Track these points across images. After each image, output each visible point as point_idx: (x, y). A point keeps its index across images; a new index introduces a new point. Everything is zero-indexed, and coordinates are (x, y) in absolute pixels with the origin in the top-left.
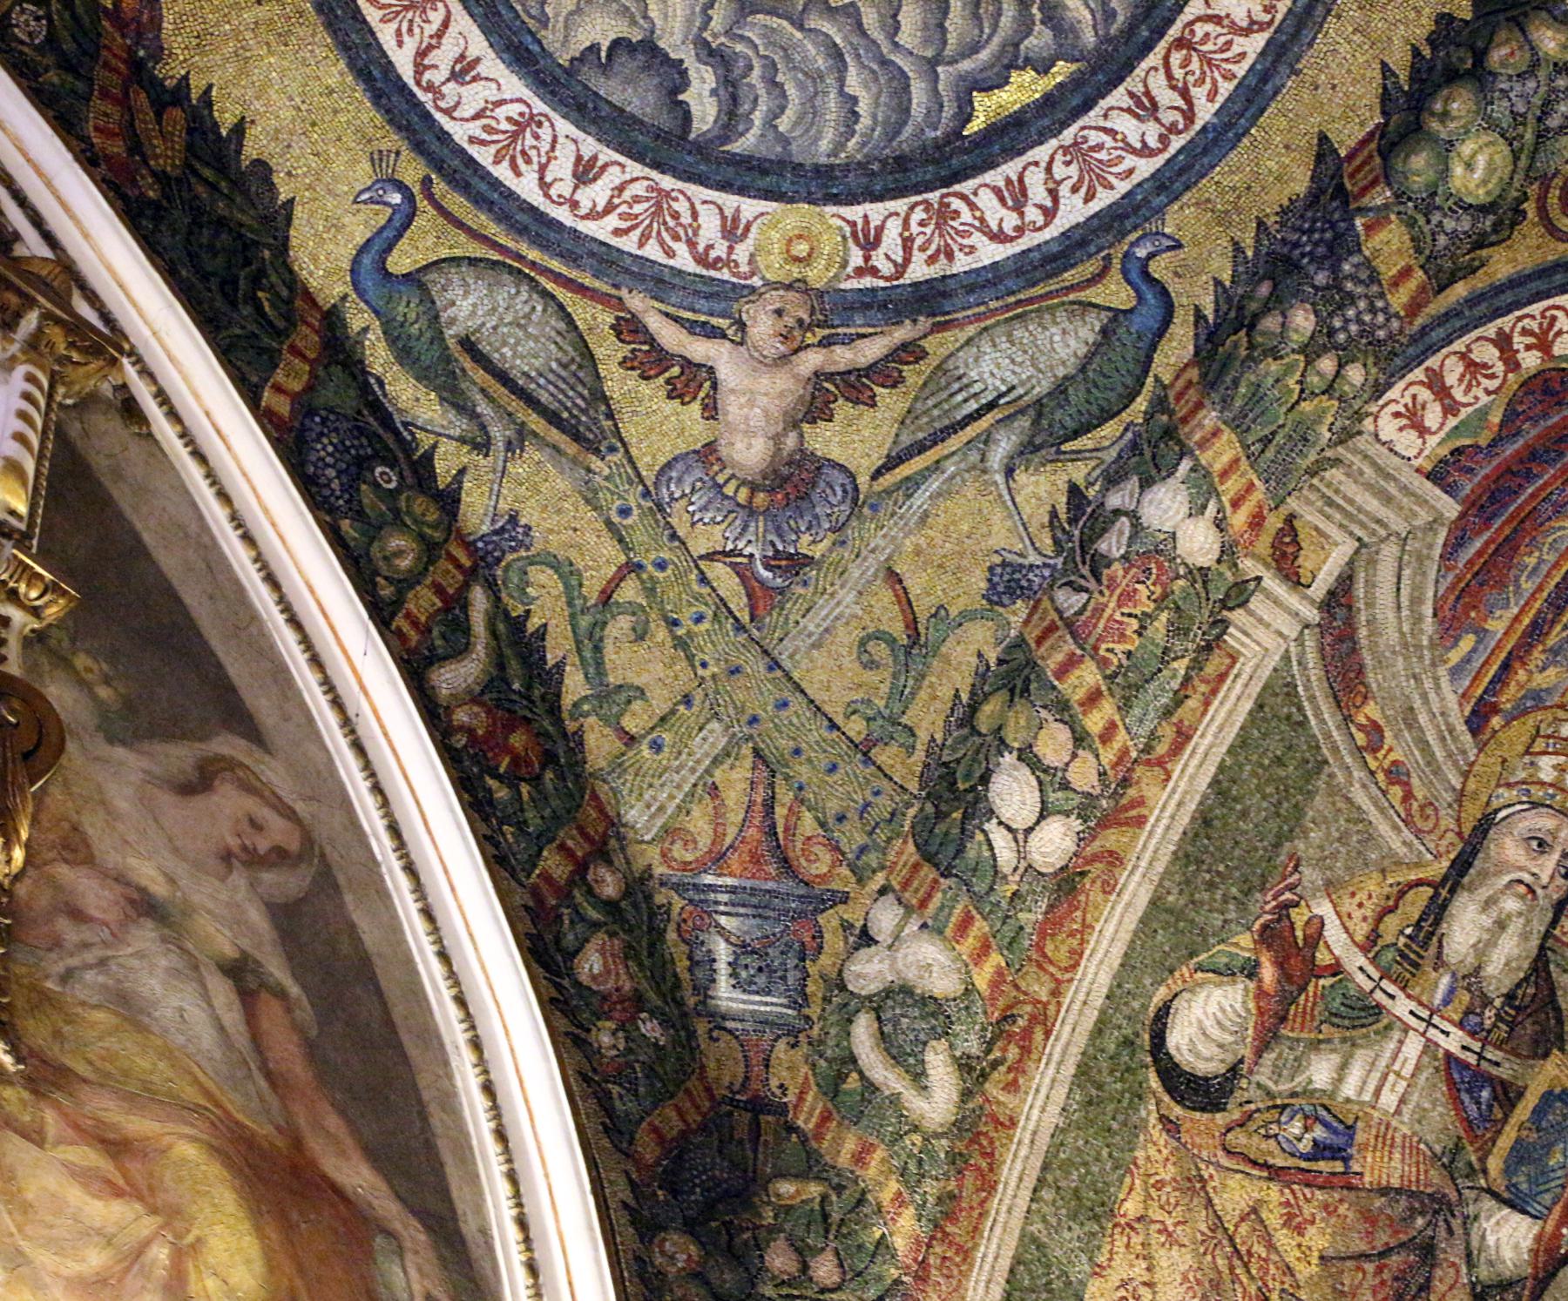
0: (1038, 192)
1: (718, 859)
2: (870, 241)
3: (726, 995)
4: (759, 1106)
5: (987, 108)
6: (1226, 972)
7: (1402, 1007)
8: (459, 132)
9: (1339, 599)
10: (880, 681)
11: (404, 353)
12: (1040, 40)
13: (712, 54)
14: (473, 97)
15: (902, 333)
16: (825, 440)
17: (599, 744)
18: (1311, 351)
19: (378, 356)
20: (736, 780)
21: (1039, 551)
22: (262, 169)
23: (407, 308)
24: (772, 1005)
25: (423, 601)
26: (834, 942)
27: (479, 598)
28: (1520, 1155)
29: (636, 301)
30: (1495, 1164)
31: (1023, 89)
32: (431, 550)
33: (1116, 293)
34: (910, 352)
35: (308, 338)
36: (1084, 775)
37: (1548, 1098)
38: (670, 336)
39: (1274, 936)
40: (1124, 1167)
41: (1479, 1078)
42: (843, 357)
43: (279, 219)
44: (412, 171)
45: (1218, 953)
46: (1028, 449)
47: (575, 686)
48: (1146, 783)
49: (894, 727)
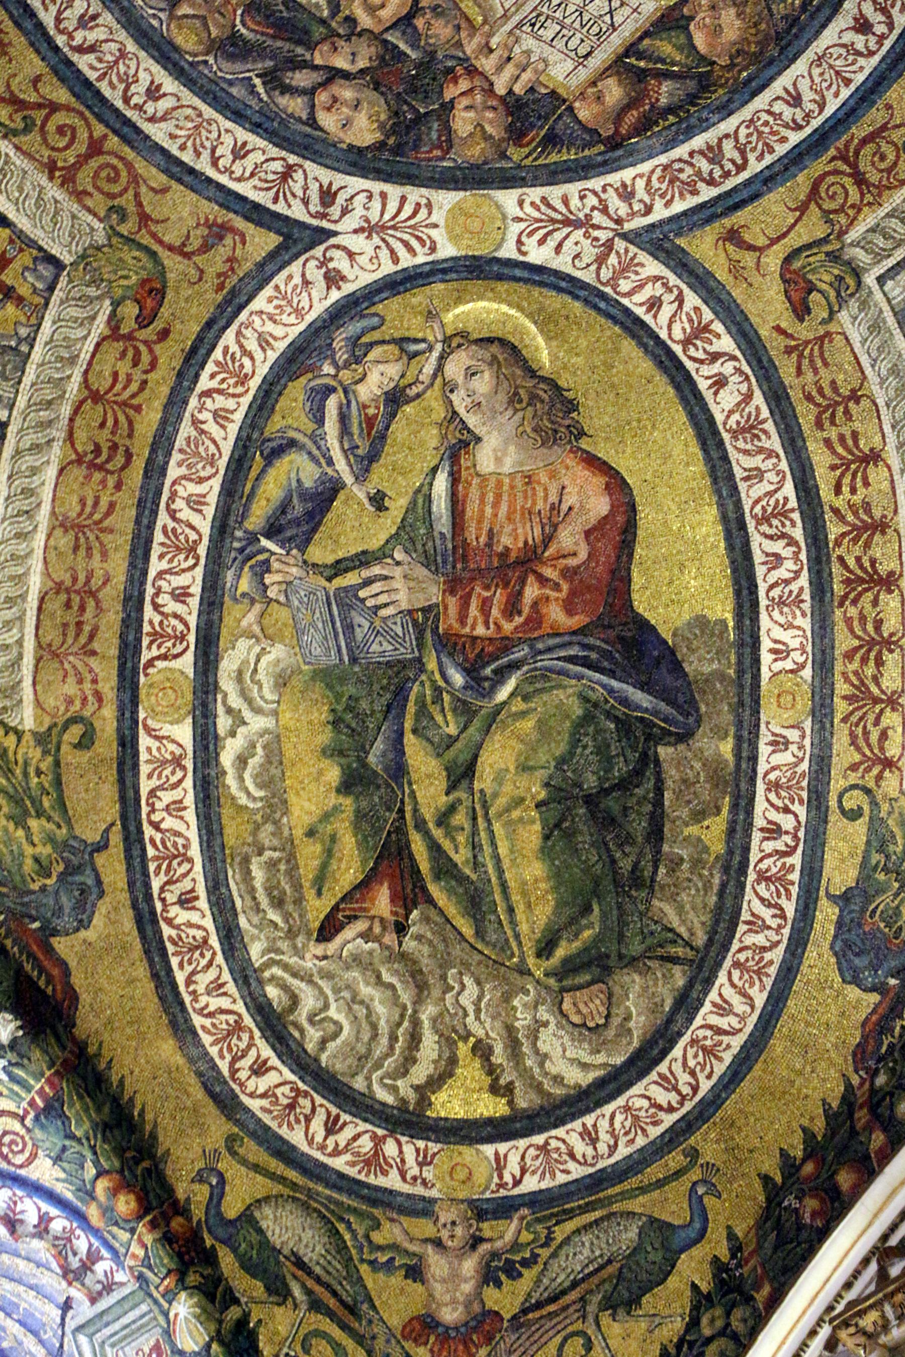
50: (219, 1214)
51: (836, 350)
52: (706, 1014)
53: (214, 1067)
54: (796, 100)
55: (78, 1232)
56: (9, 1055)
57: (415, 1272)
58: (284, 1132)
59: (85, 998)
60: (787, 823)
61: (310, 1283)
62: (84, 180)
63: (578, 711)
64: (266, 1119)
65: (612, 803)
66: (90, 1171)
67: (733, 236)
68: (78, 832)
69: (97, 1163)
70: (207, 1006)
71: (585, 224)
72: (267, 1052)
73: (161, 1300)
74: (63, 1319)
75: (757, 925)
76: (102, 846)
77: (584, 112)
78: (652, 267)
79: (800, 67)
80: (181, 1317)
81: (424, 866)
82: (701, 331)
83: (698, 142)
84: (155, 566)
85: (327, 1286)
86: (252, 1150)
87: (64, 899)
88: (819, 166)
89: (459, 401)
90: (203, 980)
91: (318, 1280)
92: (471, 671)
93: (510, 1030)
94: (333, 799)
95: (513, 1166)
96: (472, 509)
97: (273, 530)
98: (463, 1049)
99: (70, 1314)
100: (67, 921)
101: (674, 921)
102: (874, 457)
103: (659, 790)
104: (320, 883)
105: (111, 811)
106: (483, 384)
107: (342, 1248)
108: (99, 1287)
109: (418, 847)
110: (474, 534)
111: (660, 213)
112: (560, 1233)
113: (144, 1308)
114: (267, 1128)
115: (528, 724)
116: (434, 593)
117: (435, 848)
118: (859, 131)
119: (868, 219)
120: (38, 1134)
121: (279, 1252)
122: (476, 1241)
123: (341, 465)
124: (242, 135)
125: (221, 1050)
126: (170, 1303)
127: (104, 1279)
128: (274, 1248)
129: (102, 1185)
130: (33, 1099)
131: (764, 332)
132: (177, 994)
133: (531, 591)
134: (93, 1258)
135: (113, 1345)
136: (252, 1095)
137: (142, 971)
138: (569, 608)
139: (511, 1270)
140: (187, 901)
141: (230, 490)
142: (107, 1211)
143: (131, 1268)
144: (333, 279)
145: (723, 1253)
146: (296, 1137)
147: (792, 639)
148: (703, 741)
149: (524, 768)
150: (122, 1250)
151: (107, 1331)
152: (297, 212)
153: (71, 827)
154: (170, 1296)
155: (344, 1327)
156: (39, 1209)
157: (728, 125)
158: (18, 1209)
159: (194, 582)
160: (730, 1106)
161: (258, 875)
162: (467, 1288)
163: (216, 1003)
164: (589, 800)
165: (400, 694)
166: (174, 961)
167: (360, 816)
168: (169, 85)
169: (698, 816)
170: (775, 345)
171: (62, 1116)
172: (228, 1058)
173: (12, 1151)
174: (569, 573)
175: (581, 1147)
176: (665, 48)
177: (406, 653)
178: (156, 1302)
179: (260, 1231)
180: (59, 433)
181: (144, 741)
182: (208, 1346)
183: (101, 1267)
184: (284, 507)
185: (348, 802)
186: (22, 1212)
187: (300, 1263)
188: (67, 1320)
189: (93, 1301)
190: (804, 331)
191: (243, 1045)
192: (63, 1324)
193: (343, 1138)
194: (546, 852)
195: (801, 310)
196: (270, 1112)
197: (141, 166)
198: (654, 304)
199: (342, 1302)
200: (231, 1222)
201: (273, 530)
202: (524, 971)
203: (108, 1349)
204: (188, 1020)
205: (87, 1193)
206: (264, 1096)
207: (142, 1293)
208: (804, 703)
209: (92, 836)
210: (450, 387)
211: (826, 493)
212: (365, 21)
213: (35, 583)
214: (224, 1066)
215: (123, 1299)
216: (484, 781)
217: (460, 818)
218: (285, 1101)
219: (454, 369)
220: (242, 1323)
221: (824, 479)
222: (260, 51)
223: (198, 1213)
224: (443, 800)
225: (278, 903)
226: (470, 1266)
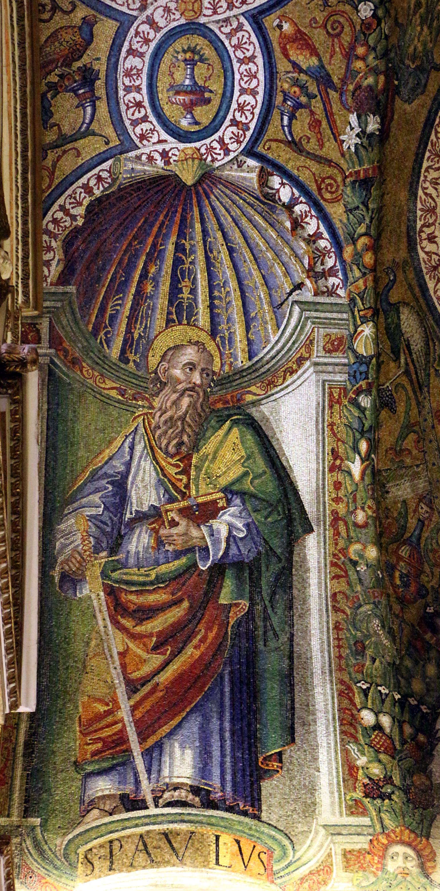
50: (387, 296)
53: (415, 221)
55: (332, 254)
56: (364, 140)
58: (427, 277)
61: (409, 360)
64: (423, 265)
66: (362, 229)
68: (435, 50)
69: (368, 227)
70: (427, 188)
73: (358, 319)
74: (292, 292)
80: (365, 333)
85: (415, 367)
87: (411, 80)
91: (413, 361)
99: (297, 292)
100: (405, 91)
108: (325, 289)
113: (345, 316)
114: (421, 271)
120: (348, 190)
121: (403, 335)
125: (422, 215)
126: (362, 323)
127: (330, 288)
128: (401, 331)
129: (363, 241)
130: (359, 171)
132: (420, 172)
134: (332, 272)
135: (313, 323)
136: (422, 248)
142: (357, 256)
143: (350, 292)
150: (351, 280)
151: (315, 314)
153: (434, 46)
154: (364, 320)
155: (415, 392)
156: (318, 228)
158: (306, 220)
166: (427, 154)
171: (368, 191)
172: (422, 223)
173: (327, 189)
178: (354, 317)
179: (399, 317)
182: (372, 357)
183: (332, 281)
186: (307, 223)
187: (408, 346)
188: (294, 294)
189: (316, 294)
191: (431, 221)
192: (290, 294)
196: (426, 264)
199: (418, 380)
200: (390, 304)
203: (309, 323)
204: (417, 189)
205: (352, 238)
206: (427, 253)
207: (348, 309)
214: (419, 224)
215: (336, 304)
218: (434, 264)
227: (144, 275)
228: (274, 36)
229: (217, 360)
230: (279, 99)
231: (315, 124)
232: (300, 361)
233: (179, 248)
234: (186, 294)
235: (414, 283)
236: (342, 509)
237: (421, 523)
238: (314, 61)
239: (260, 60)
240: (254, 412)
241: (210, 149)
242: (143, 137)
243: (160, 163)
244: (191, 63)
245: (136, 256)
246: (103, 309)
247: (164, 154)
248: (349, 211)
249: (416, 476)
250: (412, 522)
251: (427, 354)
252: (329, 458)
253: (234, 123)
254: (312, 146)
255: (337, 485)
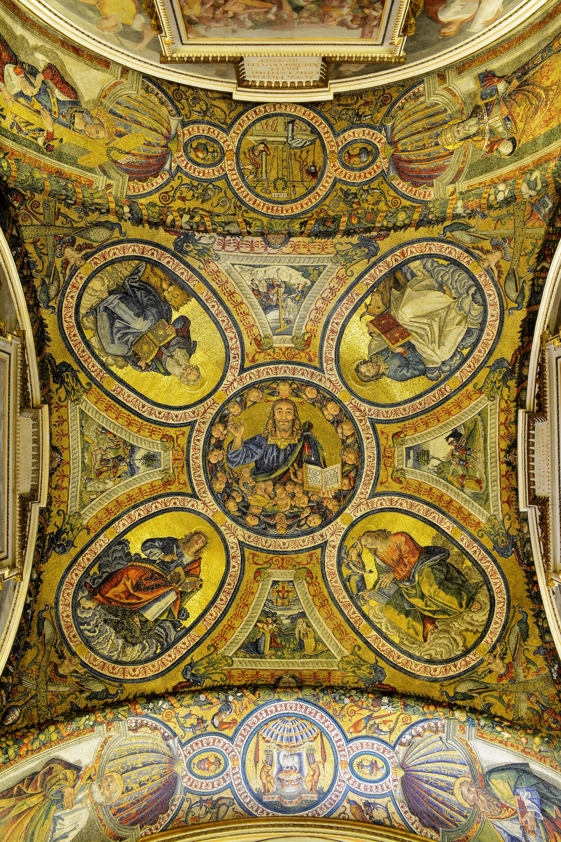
0: (448, 251)
1: (539, 219)
2: (468, 262)
3: (550, 205)
4: (557, 191)
5: (445, 263)
6: (499, 152)
7: (487, 128)
8: (499, 311)
9: (453, 182)
10: (505, 220)
11: (524, 297)
12: (435, 264)
13: (468, 294)
14: (494, 313)
15: (473, 250)
16: (489, 248)
17: (540, 242)
18: (432, 213)
19: (527, 299)
20: (529, 225)
21: (478, 216)
22: (521, 327)
23: (519, 300)
24: (546, 199)
25: (543, 275)
26: (535, 199)
27: (539, 268)
28: (492, 96)
29: (496, 279)
30: (494, 98)
31: (442, 262)
32: (538, 278)
33: (448, 234)
34: (474, 248)
35: (531, 309)
36: (492, 191)
37: (483, 99)
38: (496, 273)
39: (491, 151)
40: (528, 143)
41: (487, 110)
42: (481, 254)
43: (524, 321)
44: (506, 312)
45: (498, 156)
46: (470, 227)
47: (537, 250)
48: (488, 183)
49: (509, 214)
51: (411, 482)
52: (494, 588)
54: (370, 457)
57: (490, 672)
59: (396, 687)
60: (475, 549)
62: (285, 565)
63: (430, 569)
65: (449, 576)
67: (382, 483)
71: (361, 503)
72: (434, 666)
75: (487, 567)
76: (377, 661)
77: (345, 488)
78: (376, 499)
79: (366, 452)
81: (431, 615)
82: (391, 501)
83: (364, 476)
84: (346, 612)
86: (446, 683)
88: (382, 462)
89: (368, 546)
90: (413, 667)
92: (409, 580)
93: (468, 623)
94: (406, 620)
95: (489, 640)
96: (386, 559)
97: (359, 591)
98: (464, 633)
100: (382, 678)
101: (476, 581)
102: (431, 489)
103: (453, 566)
104: (417, 634)
105: (373, 655)
106: (370, 540)
107: (475, 681)
109: (427, 614)
110: (390, 562)
111: (369, 491)
112: (506, 640)
115: (425, 579)
116: (392, 576)
117: (429, 611)
118: (382, 451)
119: (396, 461)
122: (495, 657)
123: (360, 572)
124: (302, 538)
131: (399, 491)
133: (406, 561)
134: (436, 724)
137: (402, 674)
138: (413, 557)
139: (505, 654)
140: (399, 657)
141: (347, 591)
142: (430, 713)
144: (334, 547)
145: (532, 613)
146: (451, 674)
147: (448, 524)
148: (452, 553)
149: (431, 586)
152: (320, 542)
154: (453, 715)
157: (365, 469)
159: (354, 609)
160: (512, 595)
161: (406, 643)
162: (501, 664)
163: (418, 668)
164: (445, 579)
165: (402, 595)
167: (414, 618)
168: (285, 540)
169: (463, 563)
170: (403, 491)
174: (408, 553)
175: (496, 626)
176: (346, 468)
177: (396, 588)
180: (313, 606)
181: (369, 640)
183: (439, 725)
184: (357, 585)
185: (410, 618)
187: (471, 690)
190: (404, 484)
193: (459, 666)
194: (447, 593)
195: (401, 482)
197: (291, 556)
198: (381, 504)
201: (359, 591)
202: (461, 613)
208: (459, 530)
209: (374, 661)
210: (365, 546)
211: (430, 501)
212: (304, 506)
213: (330, 631)
216: (427, 593)
217: (429, 603)
219: (363, 542)
220: (470, 708)
221: (428, 499)
222: (294, 524)
223: (447, 700)
224: (424, 603)
225: (414, 643)
226: (498, 661)
227: (436, 799)
228: (354, 735)
229: (467, 779)
230: (376, 735)
231: (385, 722)
232: (467, 745)
233: (427, 782)
234: (443, 784)
235: (449, 682)
236: (521, 748)
237: (538, 702)
238: (363, 721)
239: (362, 741)
240: (486, 770)
241: (392, 763)
242: (388, 788)
243: (397, 783)
244: (363, 766)
245: (429, 800)
246: (447, 819)
247: (394, 780)
248: (414, 714)
249: (519, 700)
250: (536, 707)
251: (475, 681)
252: (502, 745)
253: (383, 753)
254: (392, 724)
255: (512, 746)
